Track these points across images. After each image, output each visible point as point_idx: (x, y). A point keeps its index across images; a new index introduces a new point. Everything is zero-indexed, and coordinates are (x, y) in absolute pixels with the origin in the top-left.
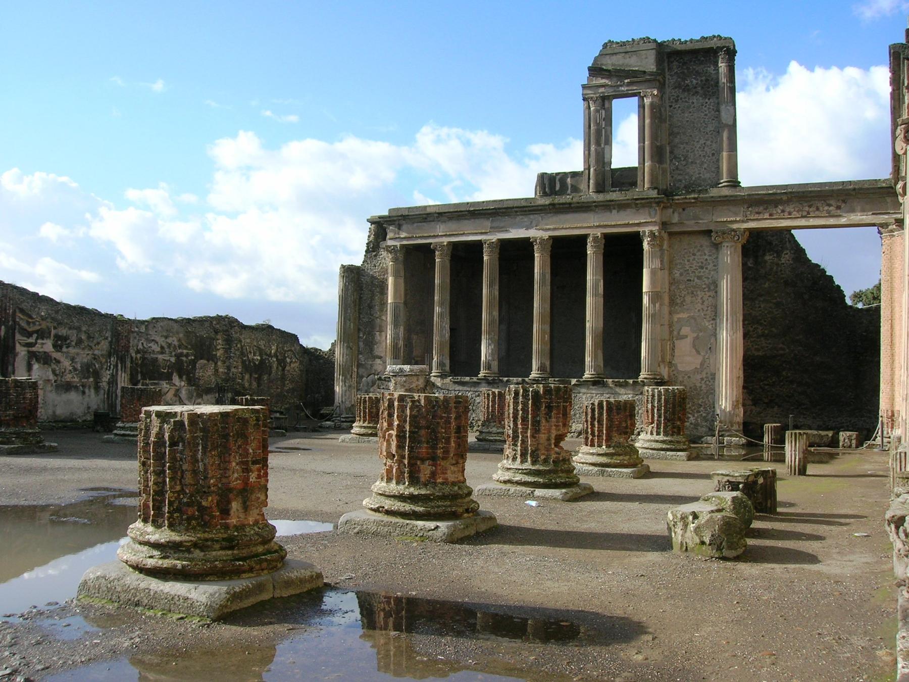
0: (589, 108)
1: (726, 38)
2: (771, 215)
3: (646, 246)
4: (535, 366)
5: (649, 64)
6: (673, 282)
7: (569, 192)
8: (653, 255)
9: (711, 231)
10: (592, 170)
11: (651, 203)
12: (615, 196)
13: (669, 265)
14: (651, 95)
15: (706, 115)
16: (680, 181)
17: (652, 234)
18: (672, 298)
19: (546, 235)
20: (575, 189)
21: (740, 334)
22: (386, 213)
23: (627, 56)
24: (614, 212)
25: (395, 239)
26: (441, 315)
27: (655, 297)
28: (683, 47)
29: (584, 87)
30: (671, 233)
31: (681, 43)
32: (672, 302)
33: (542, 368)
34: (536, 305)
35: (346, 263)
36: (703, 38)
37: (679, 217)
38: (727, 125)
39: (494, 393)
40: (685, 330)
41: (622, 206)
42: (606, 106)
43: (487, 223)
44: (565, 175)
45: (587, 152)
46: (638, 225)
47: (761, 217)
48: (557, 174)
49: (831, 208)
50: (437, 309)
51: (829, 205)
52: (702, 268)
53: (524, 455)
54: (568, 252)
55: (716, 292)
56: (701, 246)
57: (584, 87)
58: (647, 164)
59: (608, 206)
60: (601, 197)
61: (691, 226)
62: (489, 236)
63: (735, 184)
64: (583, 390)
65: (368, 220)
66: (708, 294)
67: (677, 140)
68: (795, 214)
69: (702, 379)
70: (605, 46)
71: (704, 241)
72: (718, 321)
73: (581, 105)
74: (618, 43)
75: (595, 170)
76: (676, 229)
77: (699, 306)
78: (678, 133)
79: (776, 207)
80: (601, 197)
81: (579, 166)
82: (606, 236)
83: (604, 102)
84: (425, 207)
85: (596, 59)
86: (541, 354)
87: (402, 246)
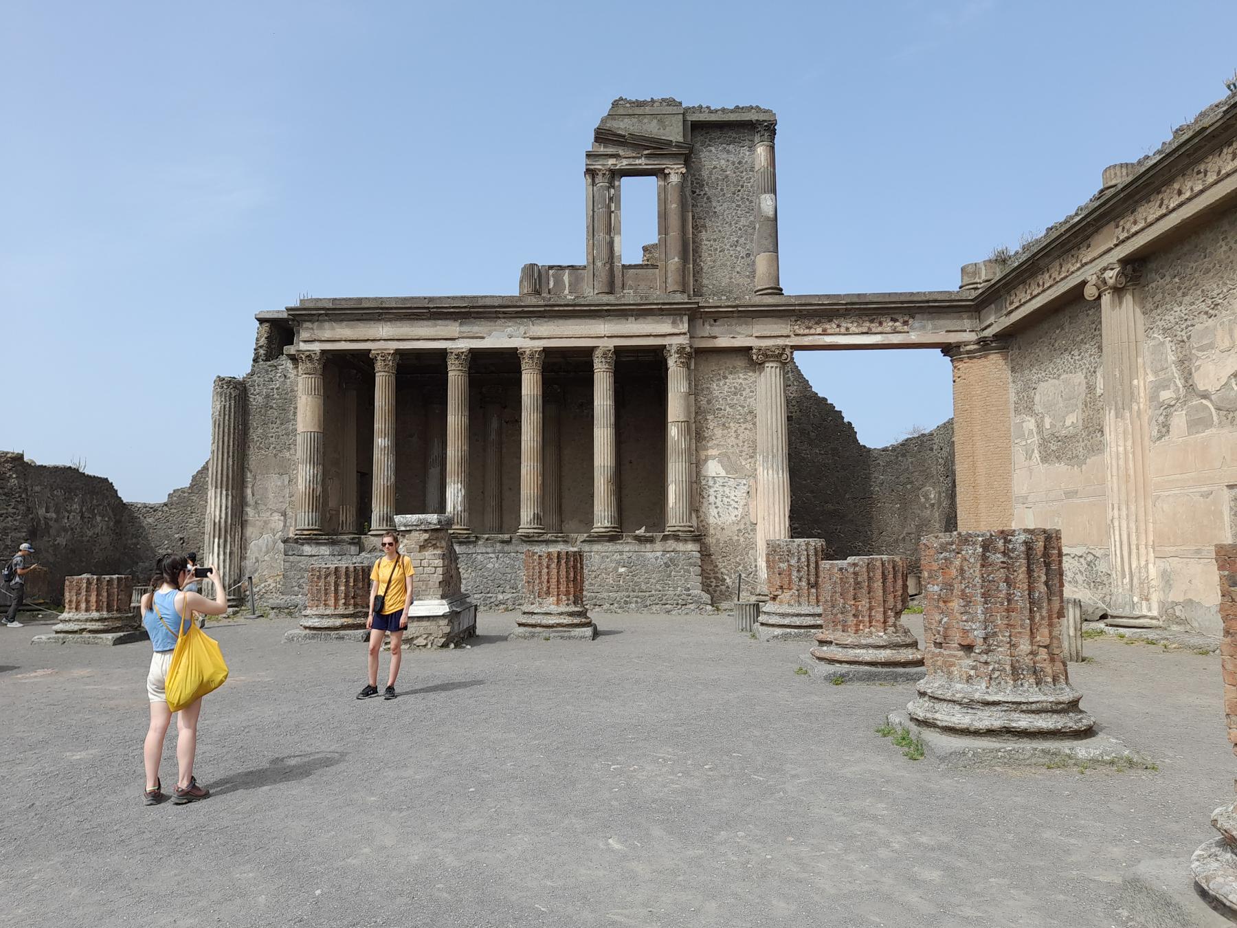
1: (766, 111)
2: (824, 330)
3: (671, 362)
4: (527, 514)
5: (674, 133)
6: (699, 411)
7: (567, 292)
9: (751, 348)
10: (599, 264)
13: (696, 390)
14: (676, 172)
15: (739, 206)
17: (681, 350)
21: (786, 476)
22: (298, 305)
24: (631, 319)
25: (314, 341)
28: (713, 118)
29: (589, 155)
31: (711, 112)
33: (538, 518)
35: (226, 374)
36: (737, 107)
38: (768, 218)
39: (549, 554)
42: (617, 183)
43: (453, 328)
44: (561, 268)
47: (812, 331)
48: (551, 267)
49: (897, 324)
50: (381, 442)
51: (895, 320)
52: (735, 394)
53: (1016, 672)
54: (567, 373)
55: (754, 424)
56: (734, 367)
57: (589, 155)
59: (621, 313)
60: (610, 299)
61: (723, 342)
62: (458, 340)
63: (779, 291)
64: (596, 547)
65: (258, 319)
66: (744, 426)
68: (853, 329)
69: (739, 530)
70: (615, 104)
71: (740, 363)
72: (759, 458)
73: (583, 182)
74: (631, 102)
77: (732, 441)
79: (830, 321)
80: (610, 299)
81: (581, 260)
82: (618, 350)
85: (603, 121)
87: (323, 352)
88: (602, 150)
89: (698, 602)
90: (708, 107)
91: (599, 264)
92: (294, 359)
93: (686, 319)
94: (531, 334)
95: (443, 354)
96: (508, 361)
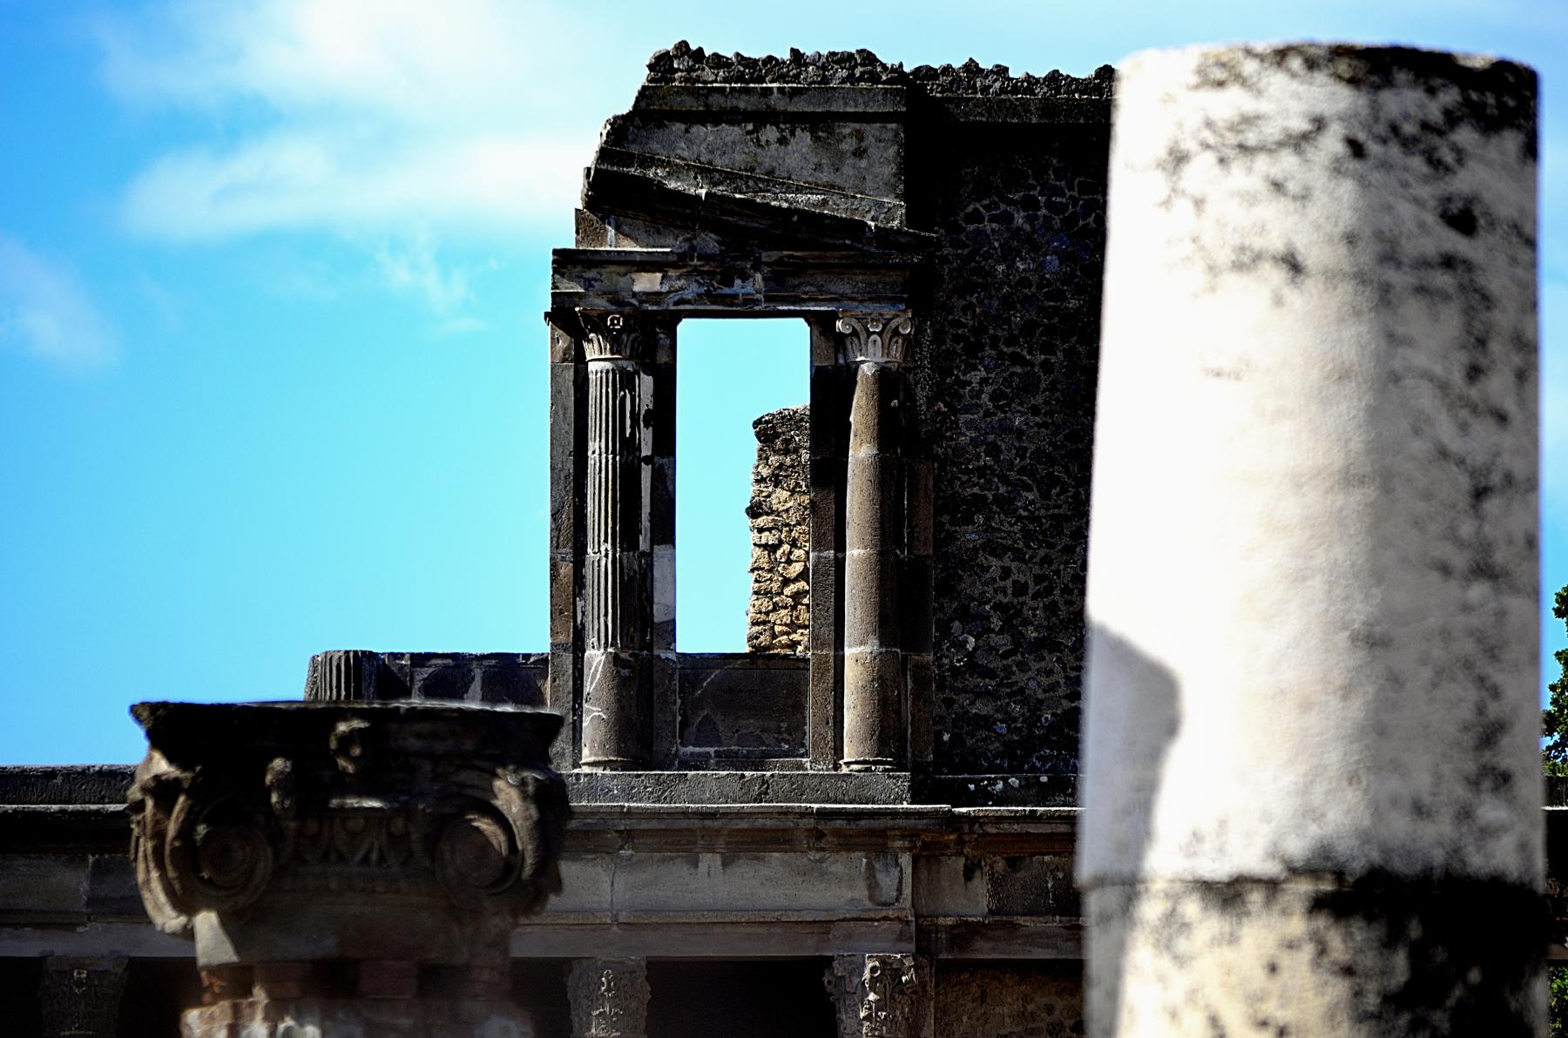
0: (580, 361)
10: (596, 657)
11: (883, 833)
12: (710, 789)
16: (986, 722)
23: (770, 133)
29: (563, 260)
37: (994, 894)
45: (566, 569)
46: (823, 927)
48: (420, 659)
57: (563, 260)
59: (680, 837)
67: (971, 536)
70: (661, 64)
73: (538, 343)
74: (718, 61)
75: (616, 660)
76: (984, 951)
78: (978, 503)
81: (529, 633)
85: (620, 129)
90: (1001, 71)
91: (596, 657)
93: (906, 860)
95: (34, 966)
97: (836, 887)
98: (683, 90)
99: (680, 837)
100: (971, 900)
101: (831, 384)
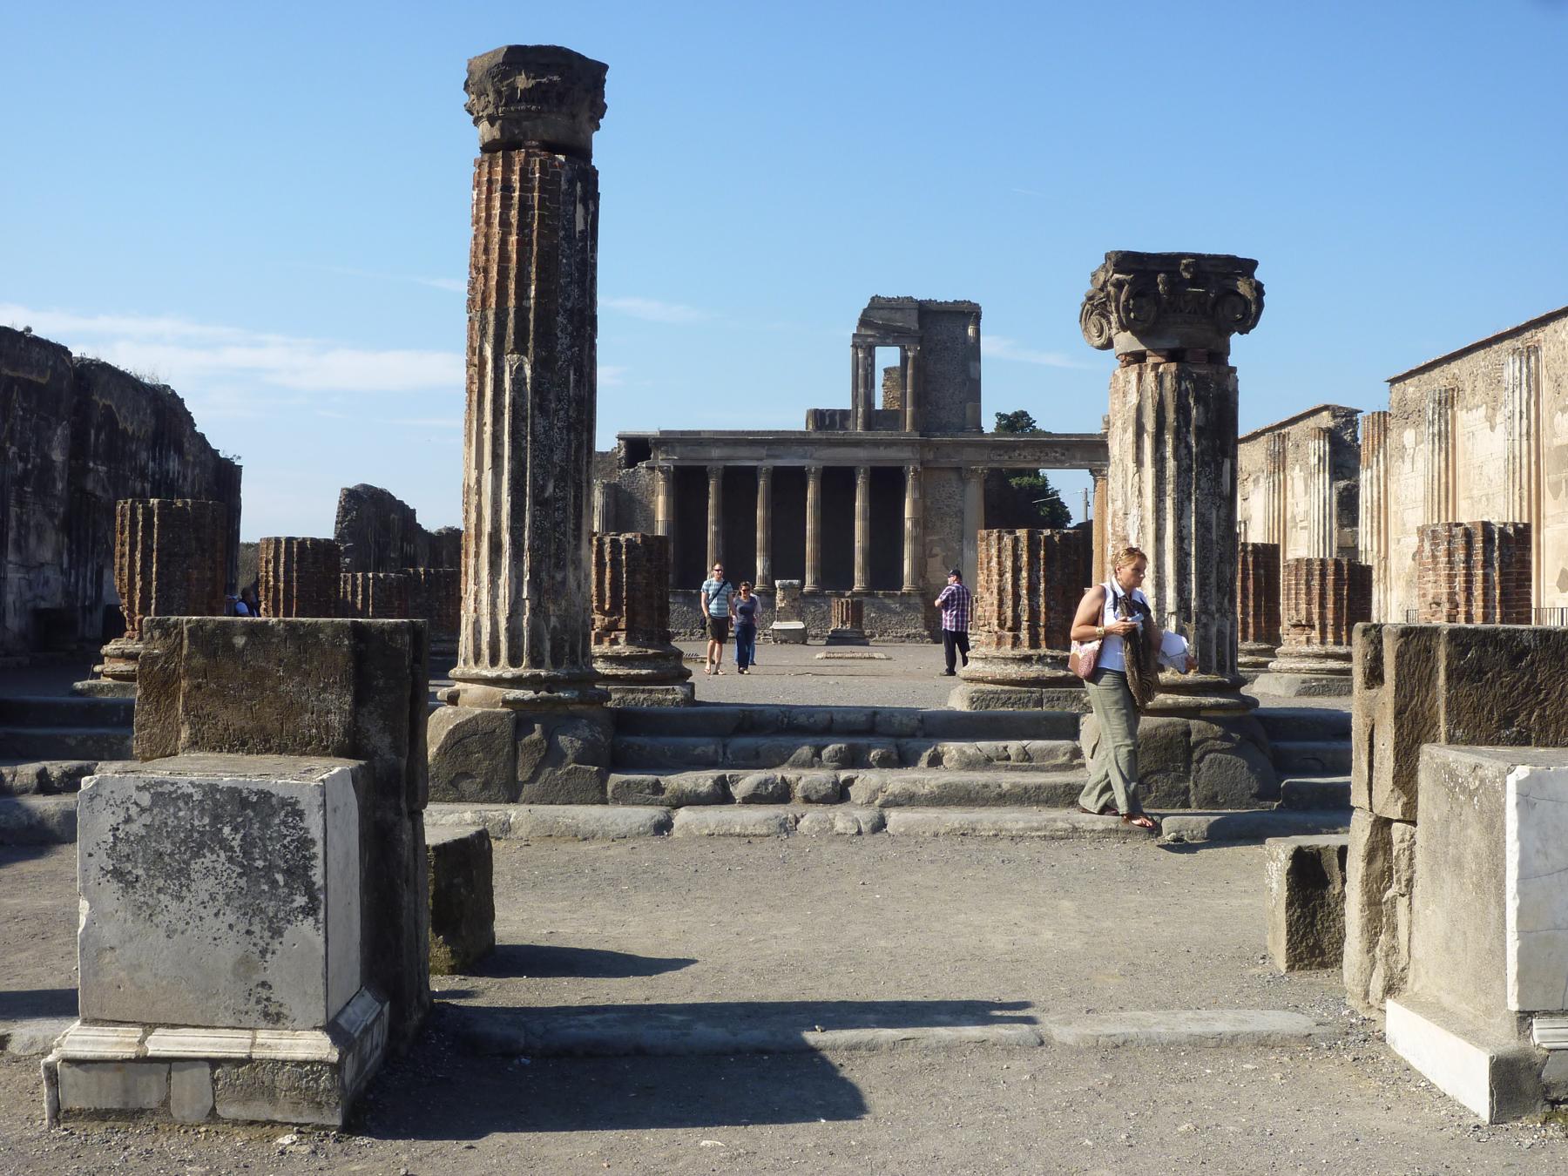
4: (809, 578)
6: (925, 508)
8: (914, 488)
12: (882, 435)
18: (922, 522)
19: (821, 465)
20: (843, 427)
26: (717, 533)
27: (916, 523)
30: (926, 468)
32: (925, 527)
33: (816, 582)
34: (809, 527)
40: (937, 550)
41: (890, 444)
43: (763, 452)
50: (712, 528)
54: (837, 482)
58: (909, 410)
59: (876, 444)
60: (869, 436)
61: (944, 463)
70: (875, 301)
71: (953, 476)
73: (850, 351)
77: (947, 530)
81: (849, 407)
83: (870, 354)
84: (699, 432)
86: (815, 569)
88: (863, 332)
89: (922, 637)
92: (652, 469)
94: (816, 455)
96: (799, 475)
97: (906, 454)
98: (877, 304)
99: (876, 444)
100: (930, 456)
101: (904, 359)
